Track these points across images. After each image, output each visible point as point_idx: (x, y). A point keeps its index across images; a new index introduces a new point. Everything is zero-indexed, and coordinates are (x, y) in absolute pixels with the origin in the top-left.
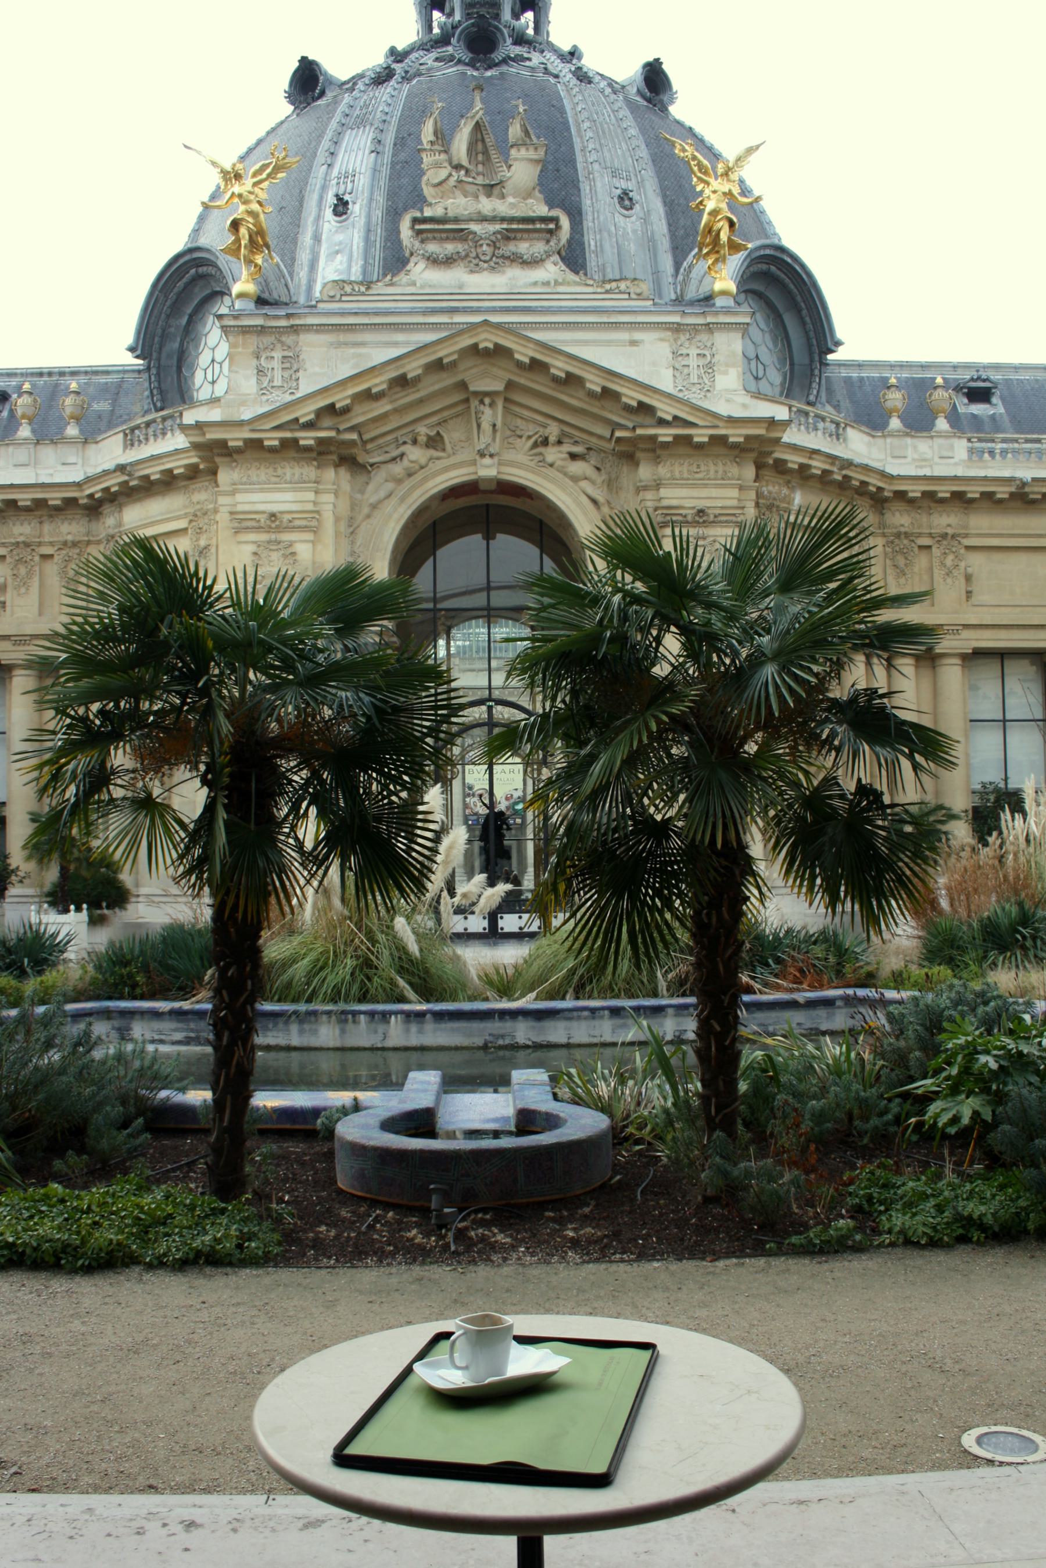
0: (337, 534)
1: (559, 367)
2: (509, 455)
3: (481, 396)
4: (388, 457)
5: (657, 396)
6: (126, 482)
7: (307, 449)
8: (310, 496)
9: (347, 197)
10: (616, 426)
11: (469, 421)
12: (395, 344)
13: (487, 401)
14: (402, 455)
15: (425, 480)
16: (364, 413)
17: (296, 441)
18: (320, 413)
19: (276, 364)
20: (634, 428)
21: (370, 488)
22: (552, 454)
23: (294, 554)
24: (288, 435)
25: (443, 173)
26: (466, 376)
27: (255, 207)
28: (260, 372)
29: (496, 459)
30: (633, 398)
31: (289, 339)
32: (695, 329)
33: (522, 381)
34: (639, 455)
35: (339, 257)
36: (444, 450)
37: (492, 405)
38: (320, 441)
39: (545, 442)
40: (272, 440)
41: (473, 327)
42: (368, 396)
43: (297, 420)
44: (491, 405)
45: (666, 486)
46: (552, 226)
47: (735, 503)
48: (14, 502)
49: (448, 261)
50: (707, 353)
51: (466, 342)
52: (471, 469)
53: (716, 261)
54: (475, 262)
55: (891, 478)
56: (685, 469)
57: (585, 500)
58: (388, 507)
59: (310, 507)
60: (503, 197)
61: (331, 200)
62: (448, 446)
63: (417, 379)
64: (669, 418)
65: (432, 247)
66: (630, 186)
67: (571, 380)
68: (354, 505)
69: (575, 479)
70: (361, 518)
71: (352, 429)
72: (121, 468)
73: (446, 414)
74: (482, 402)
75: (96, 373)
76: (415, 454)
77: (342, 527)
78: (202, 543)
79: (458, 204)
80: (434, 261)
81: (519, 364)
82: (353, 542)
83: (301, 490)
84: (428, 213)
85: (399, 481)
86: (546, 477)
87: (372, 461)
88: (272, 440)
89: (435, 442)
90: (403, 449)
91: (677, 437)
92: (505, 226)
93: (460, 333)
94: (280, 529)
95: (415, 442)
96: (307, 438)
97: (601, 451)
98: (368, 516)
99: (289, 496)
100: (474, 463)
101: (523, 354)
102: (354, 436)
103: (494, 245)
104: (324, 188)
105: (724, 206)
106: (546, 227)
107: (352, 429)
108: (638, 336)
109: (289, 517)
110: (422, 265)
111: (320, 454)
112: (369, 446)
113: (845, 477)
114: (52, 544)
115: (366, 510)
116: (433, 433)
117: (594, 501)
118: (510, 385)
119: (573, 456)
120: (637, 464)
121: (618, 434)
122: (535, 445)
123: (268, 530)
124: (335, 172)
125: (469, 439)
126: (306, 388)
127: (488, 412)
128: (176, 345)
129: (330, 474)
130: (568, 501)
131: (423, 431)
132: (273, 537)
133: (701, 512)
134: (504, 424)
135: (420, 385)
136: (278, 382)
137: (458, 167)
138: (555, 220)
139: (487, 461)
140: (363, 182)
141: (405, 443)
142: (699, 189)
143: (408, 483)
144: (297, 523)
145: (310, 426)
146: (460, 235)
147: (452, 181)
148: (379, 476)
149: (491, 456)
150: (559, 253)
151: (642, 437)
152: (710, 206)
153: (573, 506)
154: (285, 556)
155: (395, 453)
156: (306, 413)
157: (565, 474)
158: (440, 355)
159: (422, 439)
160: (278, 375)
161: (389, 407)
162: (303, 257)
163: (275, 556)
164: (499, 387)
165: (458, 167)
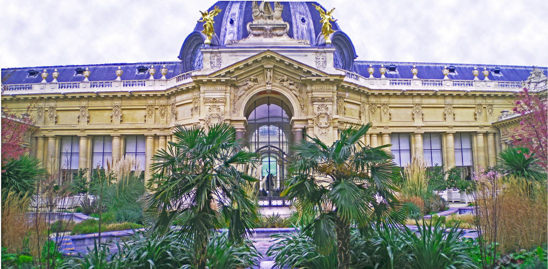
0: (230, 104)
1: (287, 62)
2: (274, 84)
3: (267, 69)
4: (243, 84)
6: (177, 90)
7: (223, 82)
8: (224, 94)
9: (233, 19)
10: (301, 77)
11: (264, 75)
12: (245, 56)
13: (269, 70)
14: (247, 84)
15: (253, 90)
17: (220, 80)
18: (226, 73)
19: (215, 61)
20: (306, 77)
21: (239, 92)
22: (285, 84)
23: (219, 108)
24: (218, 78)
25: (258, 14)
26: (263, 64)
27: (210, 21)
28: (211, 63)
31: (219, 55)
32: (322, 52)
33: (278, 65)
34: (307, 84)
35: (231, 34)
38: (226, 80)
39: (283, 81)
40: (214, 80)
41: (265, 51)
42: (238, 69)
43: (220, 75)
44: (270, 71)
45: (314, 92)
46: (285, 26)
47: (331, 96)
49: (259, 35)
51: (263, 55)
52: (265, 87)
53: (326, 35)
54: (266, 36)
55: (370, 90)
56: (319, 87)
58: (243, 97)
59: (224, 97)
60: (272, 19)
61: (229, 20)
62: (259, 82)
63: (251, 65)
65: (255, 32)
66: (304, 17)
67: (290, 65)
68: (235, 96)
69: (291, 90)
70: (236, 100)
71: (234, 77)
72: (175, 87)
73: (258, 73)
74: (267, 70)
75: (170, 63)
76: (251, 83)
77: (232, 102)
78: (196, 106)
79: (261, 21)
80: (255, 35)
81: (277, 61)
82: (234, 106)
83: (221, 92)
84: (254, 23)
85: (246, 90)
86: (284, 90)
88: (214, 80)
90: (247, 82)
91: (317, 79)
93: (262, 53)
94: (216, 102)
95: (250, 80)
96: (223, 79)
97: (297, 83)
98: (239, 99)
99: (218, 94)
100: (265, 86)
101: (278, 58)
102: (235, 79)
103: (270, 31)
104: (228, 17)
105: (328, 21)
106: (283, 28)
107: (234, 77)
108: (306, 54)
109: (219, 99)
110: (252, 36)
111: (226, 83)
113: (359, 89)
114: (158, 105)
115: (238, 98)
116: (255, 78)
117: (296, 96)
118: (274, 66)
119: (290, 84)
120: (307, 86)
121: (302, 79)
122: (281, 81)
123: (213, 102)
124: (230, 13)
125: (264, 80)
126: (222, 67)
128: (190, 56)
129: (229, 88)
131: (252, 77)
132: (214, 104)
133: (323, 98)
134: (273, 76)
136: (216, 65)
137: (261, 12)
138: (286, 25)
139: (269, 85)
140: (237, 15)
142: (322, 17)
143: (249, 91)
144: (220, 101)
145: (224, 76)
146: (262, 29)
147: (260, 15)
148: (241, 89)
149: (270, 84)
150: (287, 33)
151: (308, 79)
152: (325, 21)
153: (290, 97)
154: (217, 109)
156: (223, 73)
157: (288, 89)
158: (257, 58)
159: (252, 80)
160: (216, 63)
161: (244, 72)
162: (222, 34)
163: (215, 109)
164: (272, 67)
165: (261, 12)
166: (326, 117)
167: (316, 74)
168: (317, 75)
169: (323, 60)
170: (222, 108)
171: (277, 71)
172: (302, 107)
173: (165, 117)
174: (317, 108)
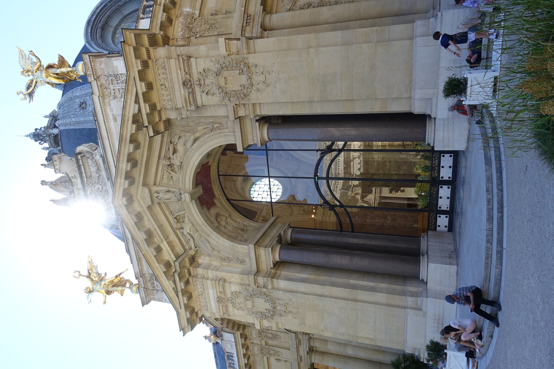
4: (191, 240)
5: (127, 114)
16: (169, 254)
22: (176, 161)
29: (182, 192)
30: (132, 127)
36: (184, 214)
39: (171, 166)
48: (244, 355)
50: (110, 78)
57: (195, 145)
64: (137, 106)
73: (167, 213)
76: (187, 228)
87: (193, 247)
92: (85, 179)
96: (181, 285)
112: (187, 248)
117: (195, 140)
119: (175, 151)
127: (161, 195)
130: (197, 154)
133: (184, 84)
135: (152, 229)
141: (182, 233)
155: (189, 237)
159: (179, 225)
161: (165, 243)
166: (225, 73)
167: (136, 102)
168: (137, 101)
169: (115, 82)
170: (235, 288)
172: (216, 126)
173: (279, 333)
174: (210, 96)
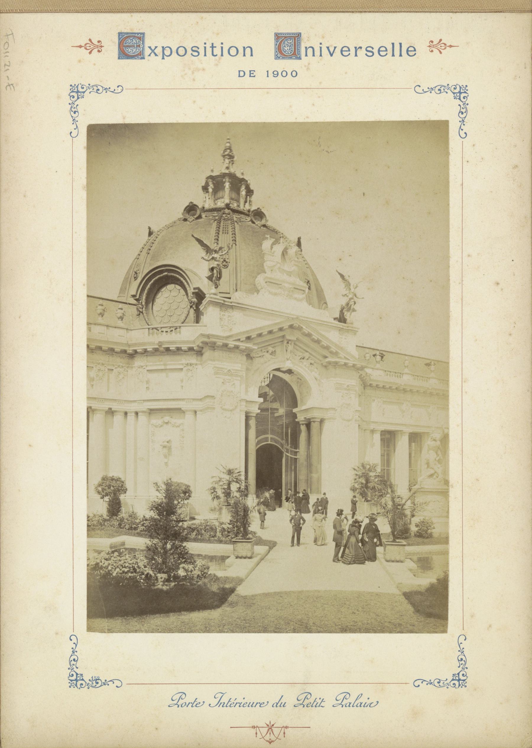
1: (315, 336)
13: (290, 342)
22: (306, 363)
37: (291, 344)
39: (303, 358)
67: (318, 342)
89: (273, 353)
95: (267, 352)
122: (301, 359)
159: (270, 352)
171: (300, 347)
